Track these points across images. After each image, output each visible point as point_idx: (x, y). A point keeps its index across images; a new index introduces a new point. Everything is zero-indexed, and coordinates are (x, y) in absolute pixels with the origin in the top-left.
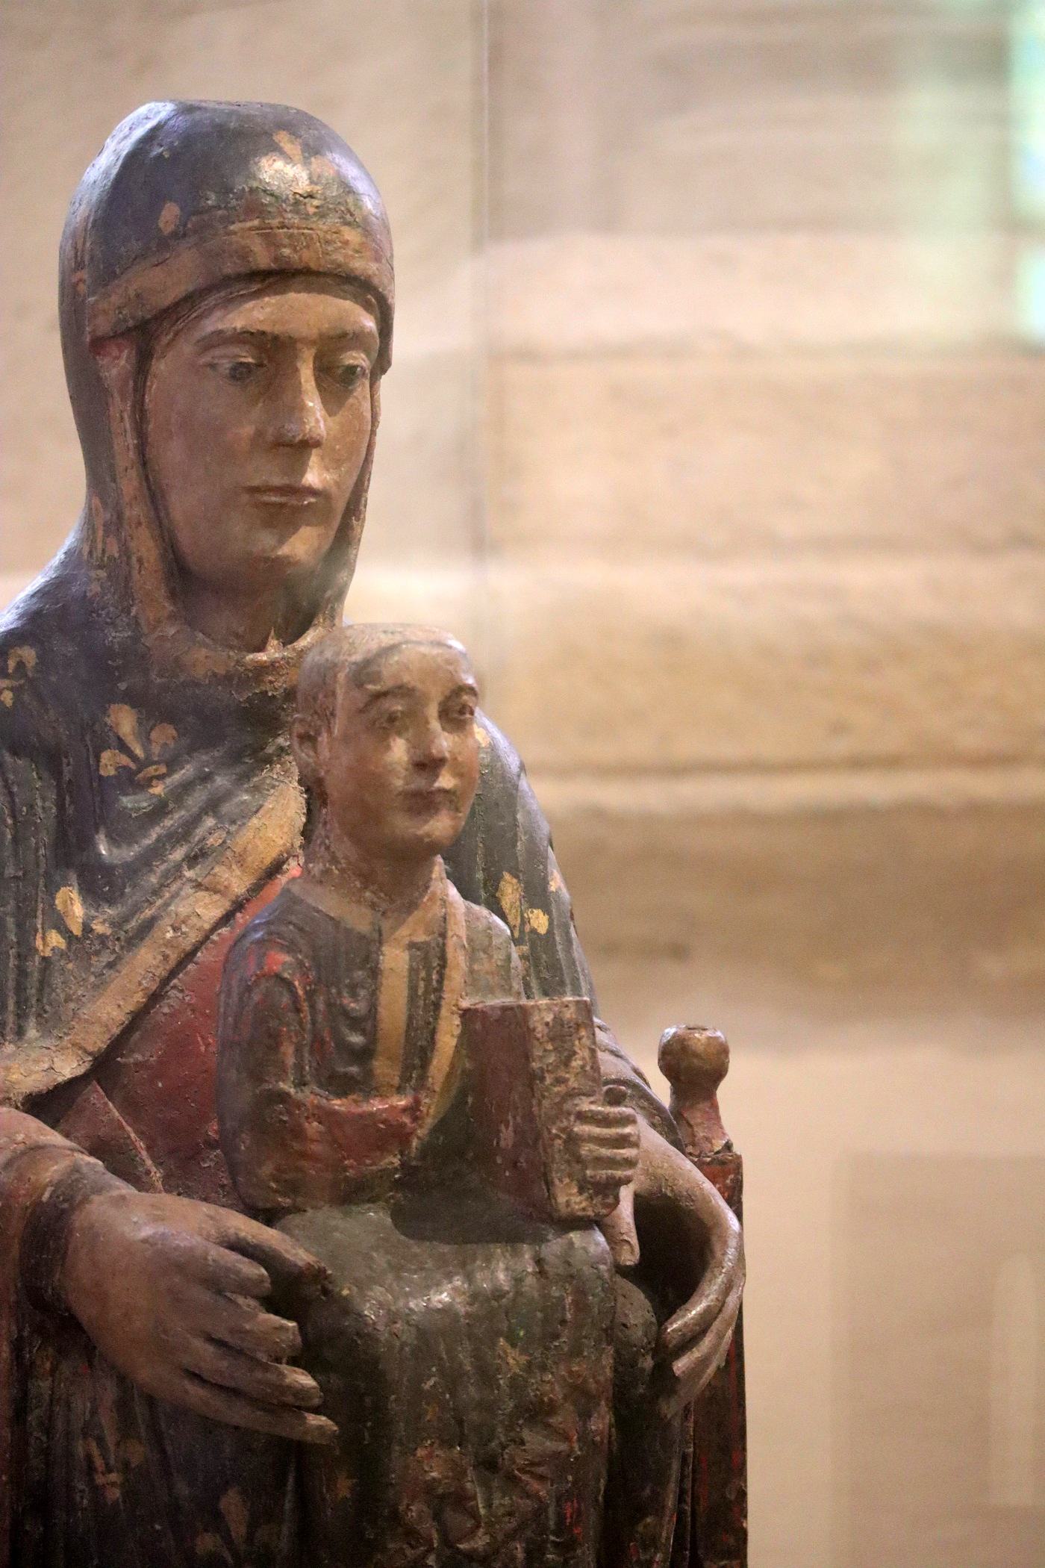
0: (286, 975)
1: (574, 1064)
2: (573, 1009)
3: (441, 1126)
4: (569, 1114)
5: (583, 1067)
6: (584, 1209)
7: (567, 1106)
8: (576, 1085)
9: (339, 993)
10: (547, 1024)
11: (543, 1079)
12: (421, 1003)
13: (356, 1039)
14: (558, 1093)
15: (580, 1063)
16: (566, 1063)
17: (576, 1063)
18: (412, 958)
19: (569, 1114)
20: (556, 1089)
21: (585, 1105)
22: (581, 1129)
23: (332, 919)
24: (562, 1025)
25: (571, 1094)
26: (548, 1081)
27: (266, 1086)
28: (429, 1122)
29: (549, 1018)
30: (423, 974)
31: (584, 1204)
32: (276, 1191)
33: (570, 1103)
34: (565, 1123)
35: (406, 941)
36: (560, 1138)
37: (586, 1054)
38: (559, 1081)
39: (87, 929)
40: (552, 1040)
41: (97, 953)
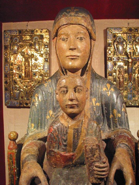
0: (52, 133)
1: (95, 156)
2: (95, 146)
3: (79, 158)
4: (94, 165)
5: (97, 157)
6: (96, 182)
7: (93, 164)
8: (95, 160)
9: (62, 136)
10: (90, 149)
11: (88, 159)
12: (76, 138)
13: (65, 143)
14: (91, 162)
15: (96, 156)
16: (93, 156)
17: (95, 156)
18: (74, 131)
19: (94, 165)
20: (91, 161)
21: (97, 164)
22: (95, 168)
23: (62, 124)
24: (93, 149)
25: (94, 162)
26: (89, 159)
27: (51, 149)
28: (77, 158)
29: (90, 148)
30: (76, 134)
31: (96, 181)
32: (53, 165)
33: (94, 163)
34: (92, 167)
35: (73, 128)
36: (91, 169)
37: (98, 154)
38: (92, 159)
39: (52, 116)
40: (91, 152)
41: (52, 119)
